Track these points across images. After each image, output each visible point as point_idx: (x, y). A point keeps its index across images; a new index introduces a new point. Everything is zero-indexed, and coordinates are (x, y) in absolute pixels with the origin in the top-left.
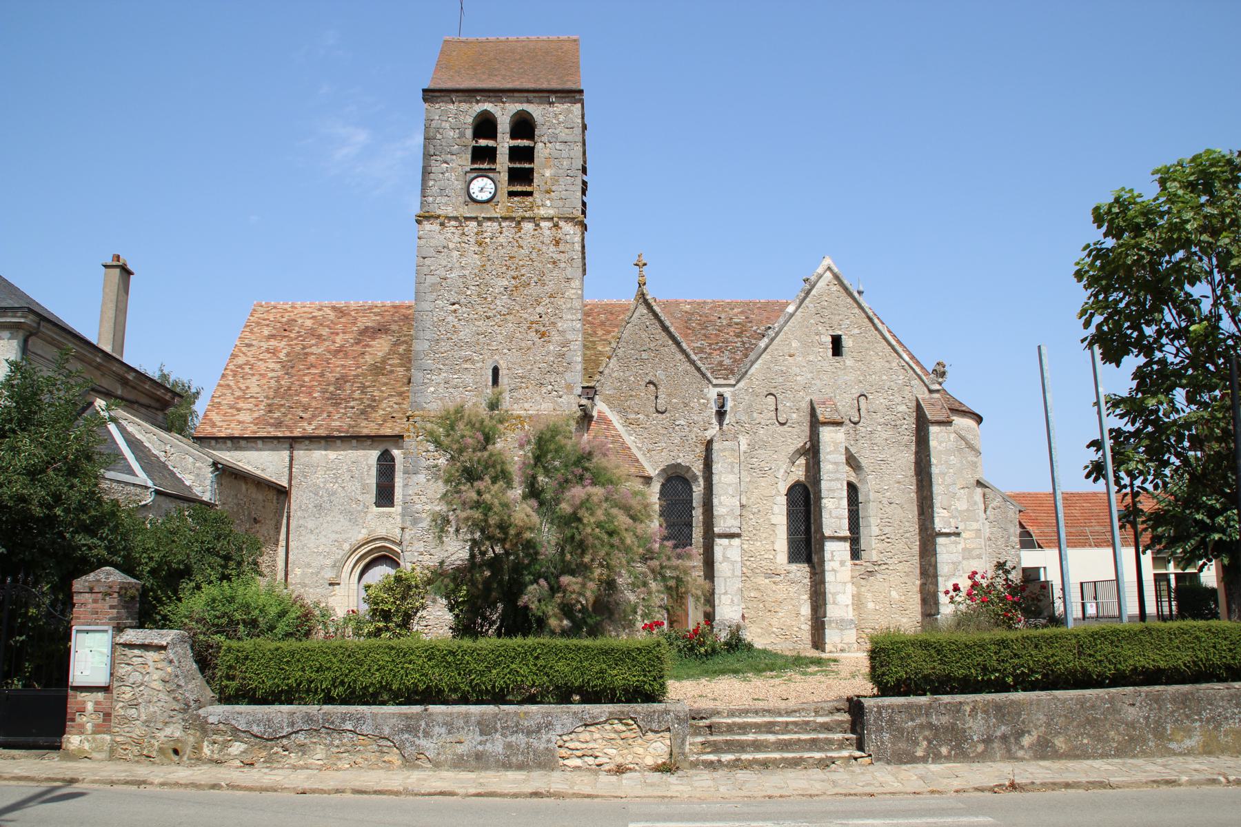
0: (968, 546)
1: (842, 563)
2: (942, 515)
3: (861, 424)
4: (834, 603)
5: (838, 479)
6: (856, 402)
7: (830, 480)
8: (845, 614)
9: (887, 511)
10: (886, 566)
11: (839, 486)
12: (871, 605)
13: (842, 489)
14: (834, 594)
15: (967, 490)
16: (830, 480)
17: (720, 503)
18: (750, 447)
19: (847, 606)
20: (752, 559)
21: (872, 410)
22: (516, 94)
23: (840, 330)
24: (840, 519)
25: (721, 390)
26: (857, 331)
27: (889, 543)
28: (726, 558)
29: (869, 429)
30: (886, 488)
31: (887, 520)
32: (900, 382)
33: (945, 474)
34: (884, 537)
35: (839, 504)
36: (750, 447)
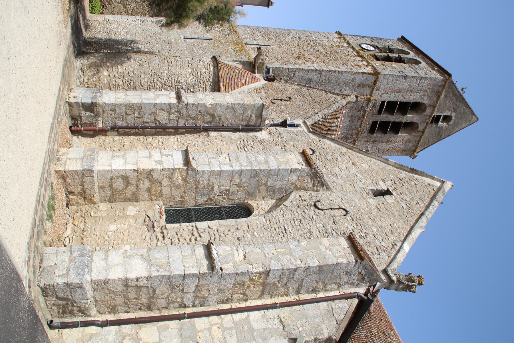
0: (200, 334)
1: (160, 162)
2: (236, 255)
3: (316, 210)
4: (113, 156)
5: (250, 163)
6: (337, 207)
7: (247, 158)
8: (100, 164)
9: (228, 236)
10: (161, 238)
11: (244, 164)
12: (113, 227)
13: (241, 166)
14: (124, 157)
15: (281, 328)
16: (247, 158)
17: (207, 95)
18: (262, 140)
19: (110, 165)
20: (160, 143)
21: (336, 220)
22: (427, 59)
23: (397, 194)
24: (209, 165)
25: (302, 125)
26: (405, 206)
27: (190, 240)
28: (159, 96)
29: (314, 217)
30: (255, 234)
31: (217, 237)
32: (378, 243)
33: (291, 254)
34: (197, 235)
35: (224, 164)
36: (262, 140)
